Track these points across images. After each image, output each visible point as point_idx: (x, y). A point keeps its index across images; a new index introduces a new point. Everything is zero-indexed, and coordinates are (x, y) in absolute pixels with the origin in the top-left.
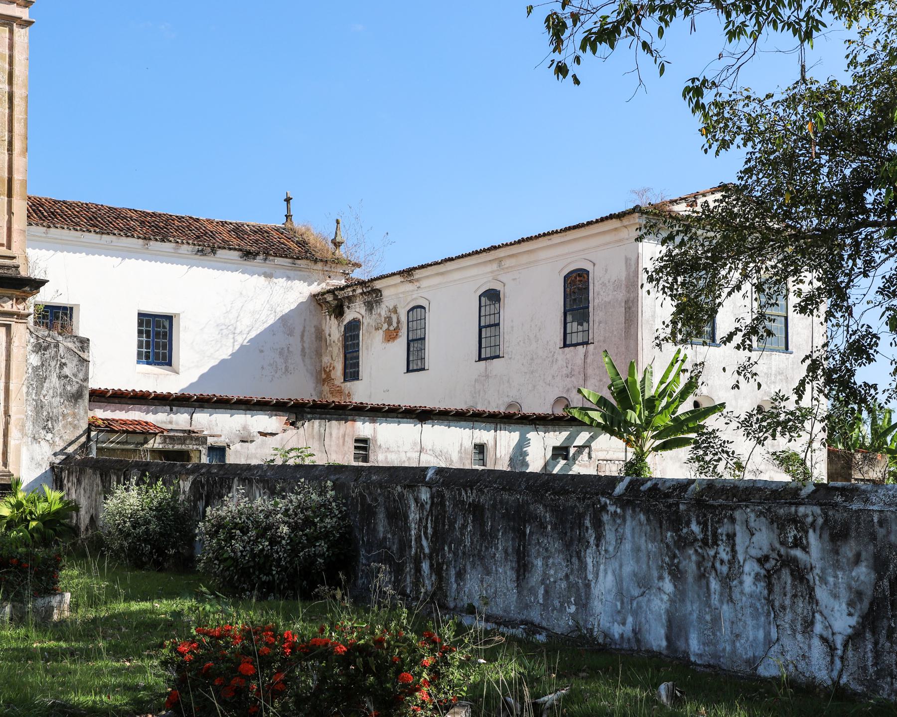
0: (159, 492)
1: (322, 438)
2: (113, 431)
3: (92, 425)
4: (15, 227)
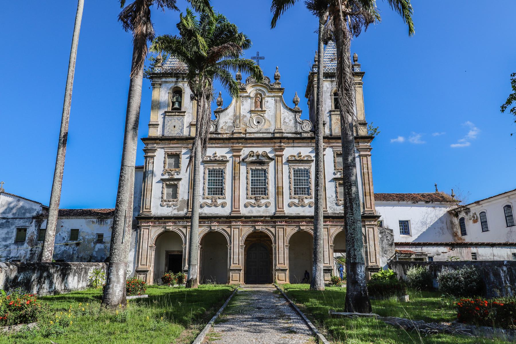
0: (421, 270)
1: (461, 253)
2: (402, 254)
3: (396, 252)
4: (372, 203)
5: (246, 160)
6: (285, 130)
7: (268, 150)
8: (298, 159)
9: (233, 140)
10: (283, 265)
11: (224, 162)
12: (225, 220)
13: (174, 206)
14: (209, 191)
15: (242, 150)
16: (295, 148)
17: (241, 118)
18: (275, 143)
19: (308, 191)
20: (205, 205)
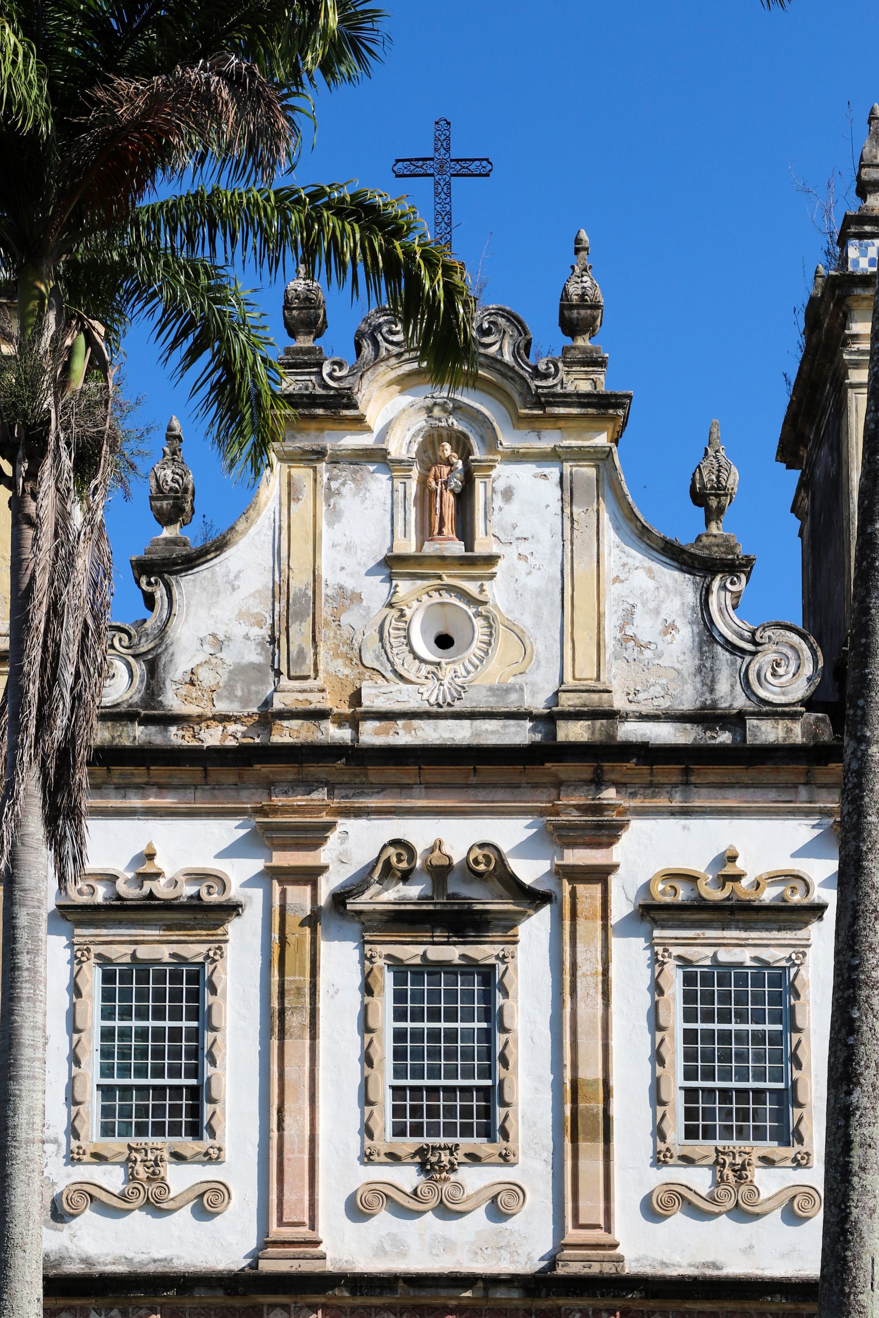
5: (361, 903)
6: (632, 695)
7: (509, 833)
8: (716, 895)
9: (277, 770)
11: (206, 914)
14: (107, 1112)
15: (333, 837)
16: (695, 824)
17: (325, 611)
18: (559, 785)
19: (781, 1116)
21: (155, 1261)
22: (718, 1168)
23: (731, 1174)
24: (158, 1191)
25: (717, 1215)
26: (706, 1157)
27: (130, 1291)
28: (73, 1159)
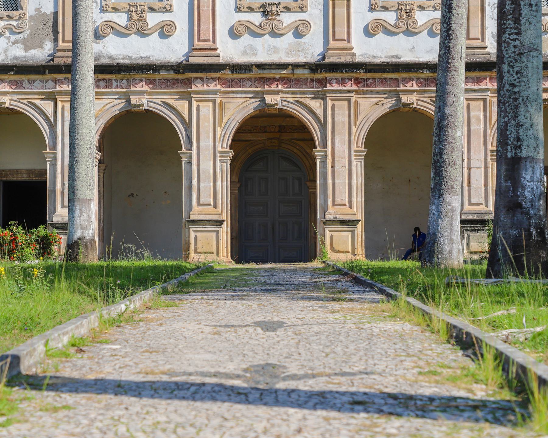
10: (346, 209)
12: (171, 75)
13: (13, 33)
20: (108, 30)
21: (142, 58)
22: (399, 11)
23: (405, 14)
24: (143, 25)
25: (398, 34)
26: (393, 6)
27: (131, 71)
28: (103, 10)
